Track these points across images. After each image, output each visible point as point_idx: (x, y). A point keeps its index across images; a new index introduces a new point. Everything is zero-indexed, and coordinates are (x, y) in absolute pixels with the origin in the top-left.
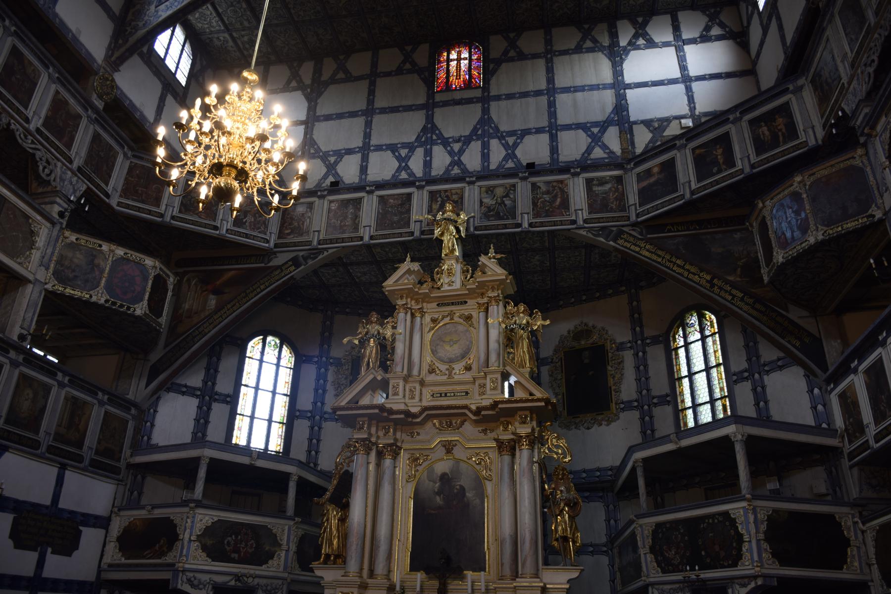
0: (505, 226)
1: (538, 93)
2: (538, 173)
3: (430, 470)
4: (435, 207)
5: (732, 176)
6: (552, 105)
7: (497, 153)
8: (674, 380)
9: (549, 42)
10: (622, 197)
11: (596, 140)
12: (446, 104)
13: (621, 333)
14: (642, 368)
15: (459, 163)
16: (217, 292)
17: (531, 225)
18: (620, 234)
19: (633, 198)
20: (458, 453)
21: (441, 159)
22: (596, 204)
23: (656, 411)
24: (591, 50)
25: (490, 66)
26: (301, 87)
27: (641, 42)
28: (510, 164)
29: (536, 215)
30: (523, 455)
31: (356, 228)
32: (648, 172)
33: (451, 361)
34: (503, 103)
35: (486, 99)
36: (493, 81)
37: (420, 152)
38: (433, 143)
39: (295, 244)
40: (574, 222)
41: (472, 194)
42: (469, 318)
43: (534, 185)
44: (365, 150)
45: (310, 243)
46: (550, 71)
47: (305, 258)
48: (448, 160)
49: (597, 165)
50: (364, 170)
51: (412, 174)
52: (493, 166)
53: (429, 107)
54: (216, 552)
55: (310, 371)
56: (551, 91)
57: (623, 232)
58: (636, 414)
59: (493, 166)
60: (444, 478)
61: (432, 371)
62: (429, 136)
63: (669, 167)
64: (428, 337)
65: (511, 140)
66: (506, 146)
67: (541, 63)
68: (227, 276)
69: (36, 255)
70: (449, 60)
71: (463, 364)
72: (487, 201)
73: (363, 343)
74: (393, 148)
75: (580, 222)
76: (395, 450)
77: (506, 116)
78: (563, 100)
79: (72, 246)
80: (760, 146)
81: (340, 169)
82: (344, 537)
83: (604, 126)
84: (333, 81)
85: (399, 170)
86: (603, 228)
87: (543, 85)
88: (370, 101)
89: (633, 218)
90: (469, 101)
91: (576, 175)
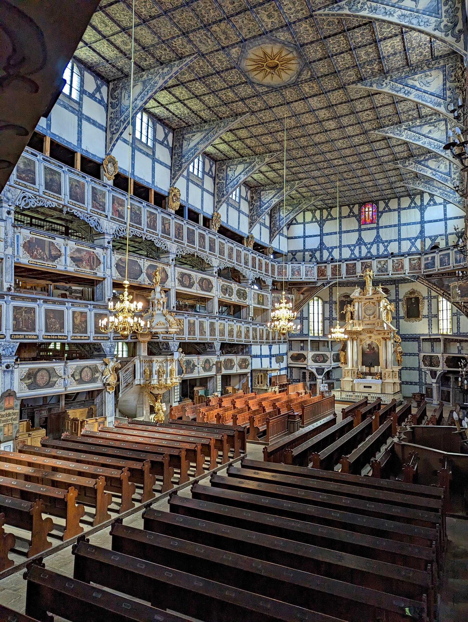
0: (384, 275)
2: (394, 256)
3: (365, 342)
4: (363, 268)
5: (448, 268)
6: (399, 230)
9: (399, 204)
11: (413, 244)
12: (365, 229)
13: (425, 294)
14: (430, 305)
15: (369, 252)
16: (302, 294)
18: (419, 277)
19: (423, 266)
21: (364, 251)
22: (412, 268)
23: (433, 319)
24: (414, 208)
26: (317, 221)
27: (432, 203)
28: (386, 253)
32: (428, 258)
33: (370, 315)
34: (384, 229)
35: (378, 228)
37: (357, 247)
39: (323, 279)
41: (375, 263)
44: (340, 247)
45: (327, 279)
46: (399, 216)
48: (367, 251)
49: (413, 254)
50: (340, 254)
51: (355, 256)
52: (380, 254)
53: (360, 230)
54: (315, 361)
55: (327, 306)
56: (399, 225)
57: (419, 277)
58: (427, 319)
59: (380, 254)
60: (369, 345)
62: (360, 241)
63: (433, 258)
64: (363, 308)
65: (386, 244)
66: (384, 246)
68: (304, 289)
69: (269, 303)
70: (365, 212)
72: (379, 266)
77: (385, 234)
78: (403, 228)
79: (274, 297)
80: (456, 262)
81: (333, 253)
83: (416, 239)
84: (327, 219)
85: (351, 254)
88: (340, 228)
90: (372, 229)
91: (406, 257)
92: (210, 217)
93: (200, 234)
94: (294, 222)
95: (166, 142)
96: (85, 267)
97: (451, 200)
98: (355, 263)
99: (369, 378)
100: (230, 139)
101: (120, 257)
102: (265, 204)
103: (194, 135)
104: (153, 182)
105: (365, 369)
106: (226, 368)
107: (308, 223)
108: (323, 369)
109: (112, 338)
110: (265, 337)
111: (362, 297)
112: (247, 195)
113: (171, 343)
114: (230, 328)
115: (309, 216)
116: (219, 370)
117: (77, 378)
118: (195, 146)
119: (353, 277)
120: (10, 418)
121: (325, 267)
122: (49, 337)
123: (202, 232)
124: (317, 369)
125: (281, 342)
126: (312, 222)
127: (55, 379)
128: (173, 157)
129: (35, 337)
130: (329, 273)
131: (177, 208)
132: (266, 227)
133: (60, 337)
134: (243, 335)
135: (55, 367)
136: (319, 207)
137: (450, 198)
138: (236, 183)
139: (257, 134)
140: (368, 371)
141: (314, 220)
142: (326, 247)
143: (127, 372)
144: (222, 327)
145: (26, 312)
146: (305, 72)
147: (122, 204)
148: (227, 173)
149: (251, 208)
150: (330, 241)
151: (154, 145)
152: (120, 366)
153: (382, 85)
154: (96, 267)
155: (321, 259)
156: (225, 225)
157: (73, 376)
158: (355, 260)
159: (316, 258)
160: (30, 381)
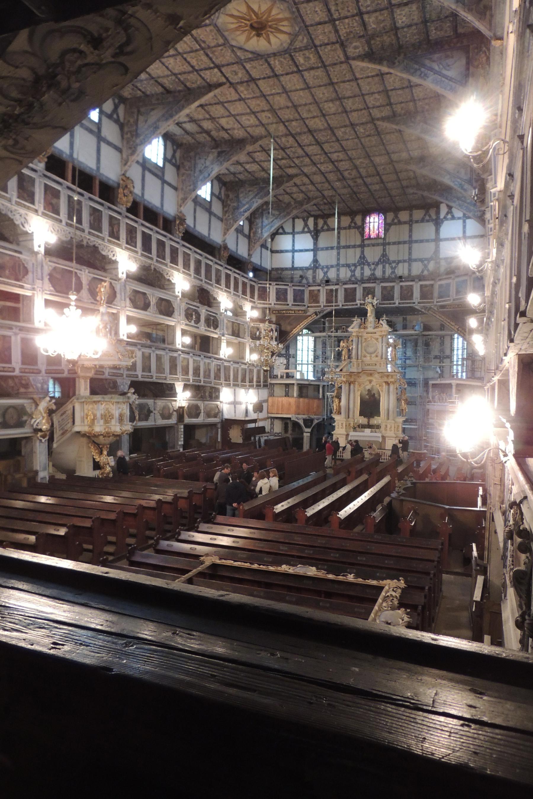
0: (390, 304)
1: (405, 242)
3: (364, 387)
6: (410, 249)
7: (388, 271)
8: (452, 350)
9: (411, 215)
10: (432, 294)
12: (369, 245)
15: (373, 274)
17: (399, 303)
20: (373, 383)
21: (367, 272)
24: (428, 221)
25: (387, 226)
26: (309, 232)
27: (449, 216)
28: (393, 276)
29: (401, 299)
30: (392, 387)
31: (336, 302)
33: (371, 354)
34: (392, 247)
36: (387, 235)
37: (359, 268)
38: (364, 264)
39: (315, 307)
40: (414, 303)
42: (377, 339)
43: (401, 287)
45: (320, 306)
46: (411, 231)
47: (320, 313)
51: (356, 279)
53: (362, 246)
56: (411, 242)
60: (369, 390)
61: (365, 356)
62: (363, 261)
66: (392, 268)
67: (407, 227)
70: (370, 223)
71: (375, 354)
72: (384, 292)
73: (342, 350)
74: (348, 266)
75: (416, 303)
76: (353, 382)
77: (393, 253)
78: (415, 246)
82: (340, 407)
84: (323, 230)
85: (352, 276)
86: (424, 306)
87: (407, 238)
88: (339, 243)
89: (435, 303)
90: (378, 245)
92: (171, 218)
93: (159, 241)
94: (281, 231)
95: (115, 116)
96: (8, 278)
97: (470, 215)
98: (355, 288)
99: (368, 431)
100: (201, 117)
101: (54, 265)
102: (244, 205)
103: (153, 109)
104: (98, 168)
105: (363, 420)
106: (190, 416)
107: (298, 233)
108: (312, 421)
109: (43, 372)
110: (240, 379)
111: (362, 330)
112: (220, 193)
113: (119, 380)
114: (195, 364)
115: (299, 224)
116: (181, 418)
118: (155, 123)
119: (353, 305)
121: (319, 290)
123: (161, 238)
124: (305, 421)
125: (260, 386)
126: (303, 232)
128: (125, 136)
130: (323, 298)
131: (129, 205)
132: (245, 236)
134: (212, 375)
136: (312, 213)
137: (470, 211)
138: (207, 175)
139: (236, 113)
140: (366, 423)
141: (306, 230)
142: (320, 265)
143: (64, 416)
144: (185, 363)
146: (300, 38)
147: (56, 194)
148: (195, 160)
149: (225, 209)
150: (327, 258)
151: (100, 119)
152: (54, 407)
153: (394, 63)
154: (23, 277)
155: (314, 281)
156: (191, 231)
158: (357, 283)
159: (307, 279)
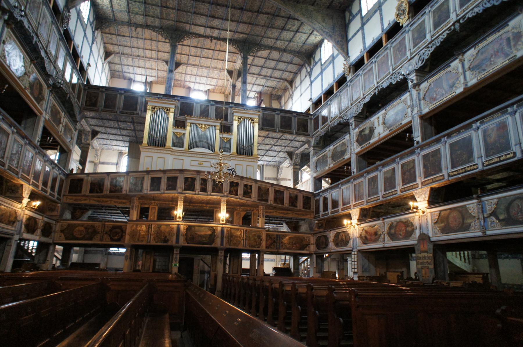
117: (501, 217)
120: (425, 261)
122: (455, 173)
127: (469, 221)
129: (441, 178)
133: (469, 169)
135: (468, 206)
145: (433, 156)
157: (494, 214)
160: (443, 224)
